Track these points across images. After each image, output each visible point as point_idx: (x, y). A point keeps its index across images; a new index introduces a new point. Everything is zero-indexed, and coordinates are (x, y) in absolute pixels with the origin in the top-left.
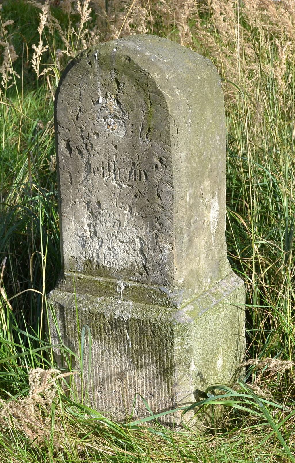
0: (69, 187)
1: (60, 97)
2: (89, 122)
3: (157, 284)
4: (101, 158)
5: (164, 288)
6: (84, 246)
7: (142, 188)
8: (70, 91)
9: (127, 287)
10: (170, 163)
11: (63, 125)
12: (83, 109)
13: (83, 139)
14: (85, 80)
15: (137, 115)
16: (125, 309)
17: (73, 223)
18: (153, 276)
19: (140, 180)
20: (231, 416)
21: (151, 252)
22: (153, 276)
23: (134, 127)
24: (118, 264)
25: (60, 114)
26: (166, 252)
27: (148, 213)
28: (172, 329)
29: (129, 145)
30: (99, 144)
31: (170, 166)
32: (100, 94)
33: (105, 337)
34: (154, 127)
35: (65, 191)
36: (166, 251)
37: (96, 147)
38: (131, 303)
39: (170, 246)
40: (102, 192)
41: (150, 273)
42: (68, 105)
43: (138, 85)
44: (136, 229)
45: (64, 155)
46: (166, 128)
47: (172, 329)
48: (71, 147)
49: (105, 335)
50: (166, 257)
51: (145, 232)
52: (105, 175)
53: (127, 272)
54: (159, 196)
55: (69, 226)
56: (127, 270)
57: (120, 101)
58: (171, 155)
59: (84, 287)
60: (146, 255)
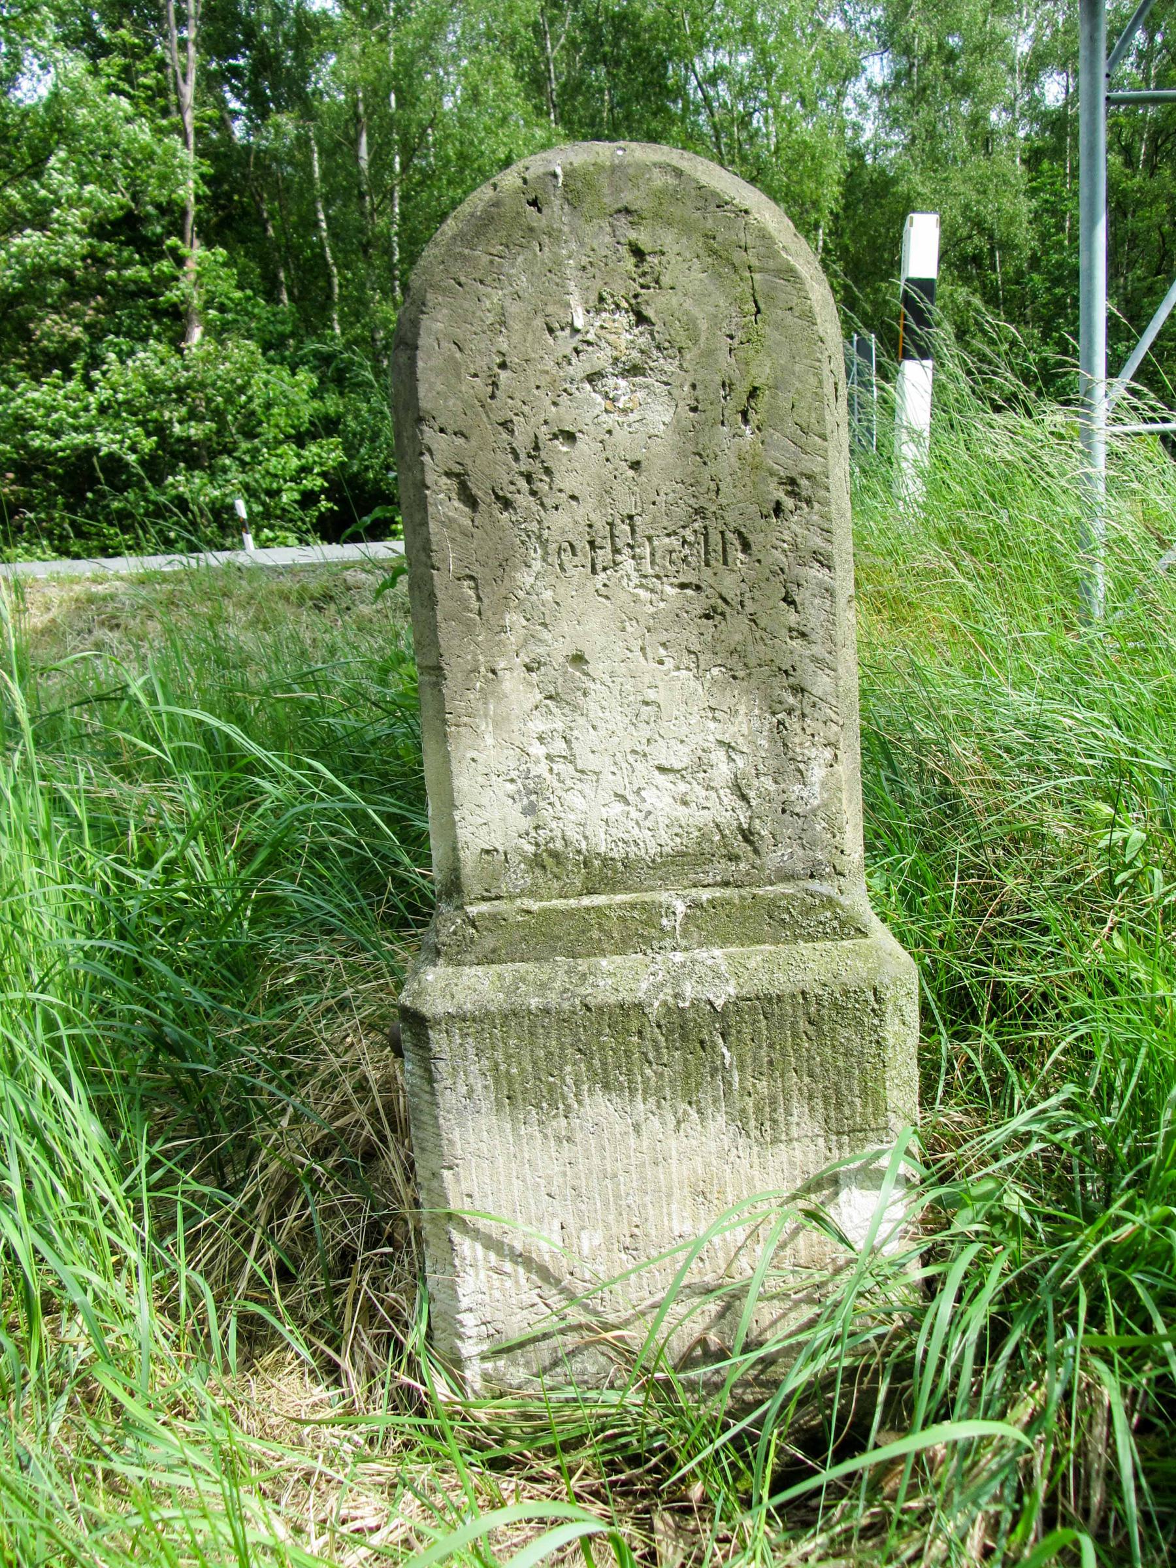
0: (469, 626)
1: (429, 329)
2: (538, 398)
3: (790, 877)
4: (585, 510)
5: (824, 888)
6: (530, 810)
7: (730, 585)
8: (466, 305)
9: (696, 905)
10: (823, 493)
11: (441, 421)
12: (513, 360)
13: (517, 459)
14: (520, 259)
15: (709, 353)
16: (719, 972)
17: (490, 741)
18: (773, 858)
19: (725, 563)
20: (992, 1219)
21: (768, 783)
22: (773, 858)
23: (699, 393)
24: (652, 841)
25: (431, 386)
26: (817, 773)
27: (752, 661)
28: (879, 1000)
29: (682, 454)
30: (575, 469)
31: (825, 503)
32: (574, 300)
33: (646, 1080)
34: (771, 382)
35: (456, 642)
36: (816, 770)
37: (568, 482)
38: (717, 952)
39: (828, 754)
40: (593, 623)
41: (763, 849)
42: (458, 355)
43: (713, 252)
44: (714, 719)
45: (449, 523)
46: (813, 381)
47: (879, 1000)
48: (474, 491)
49: (648, 1072)
50: (817, 788)
51: (746, 723)
52: (599, 567)
53: (681, 863)
54: (792, 603)
55: (474, 754)
56: (684, 854)
57: (649, 312)
58: (826, 466)
59: (545, 938)
60: (752, 794)
